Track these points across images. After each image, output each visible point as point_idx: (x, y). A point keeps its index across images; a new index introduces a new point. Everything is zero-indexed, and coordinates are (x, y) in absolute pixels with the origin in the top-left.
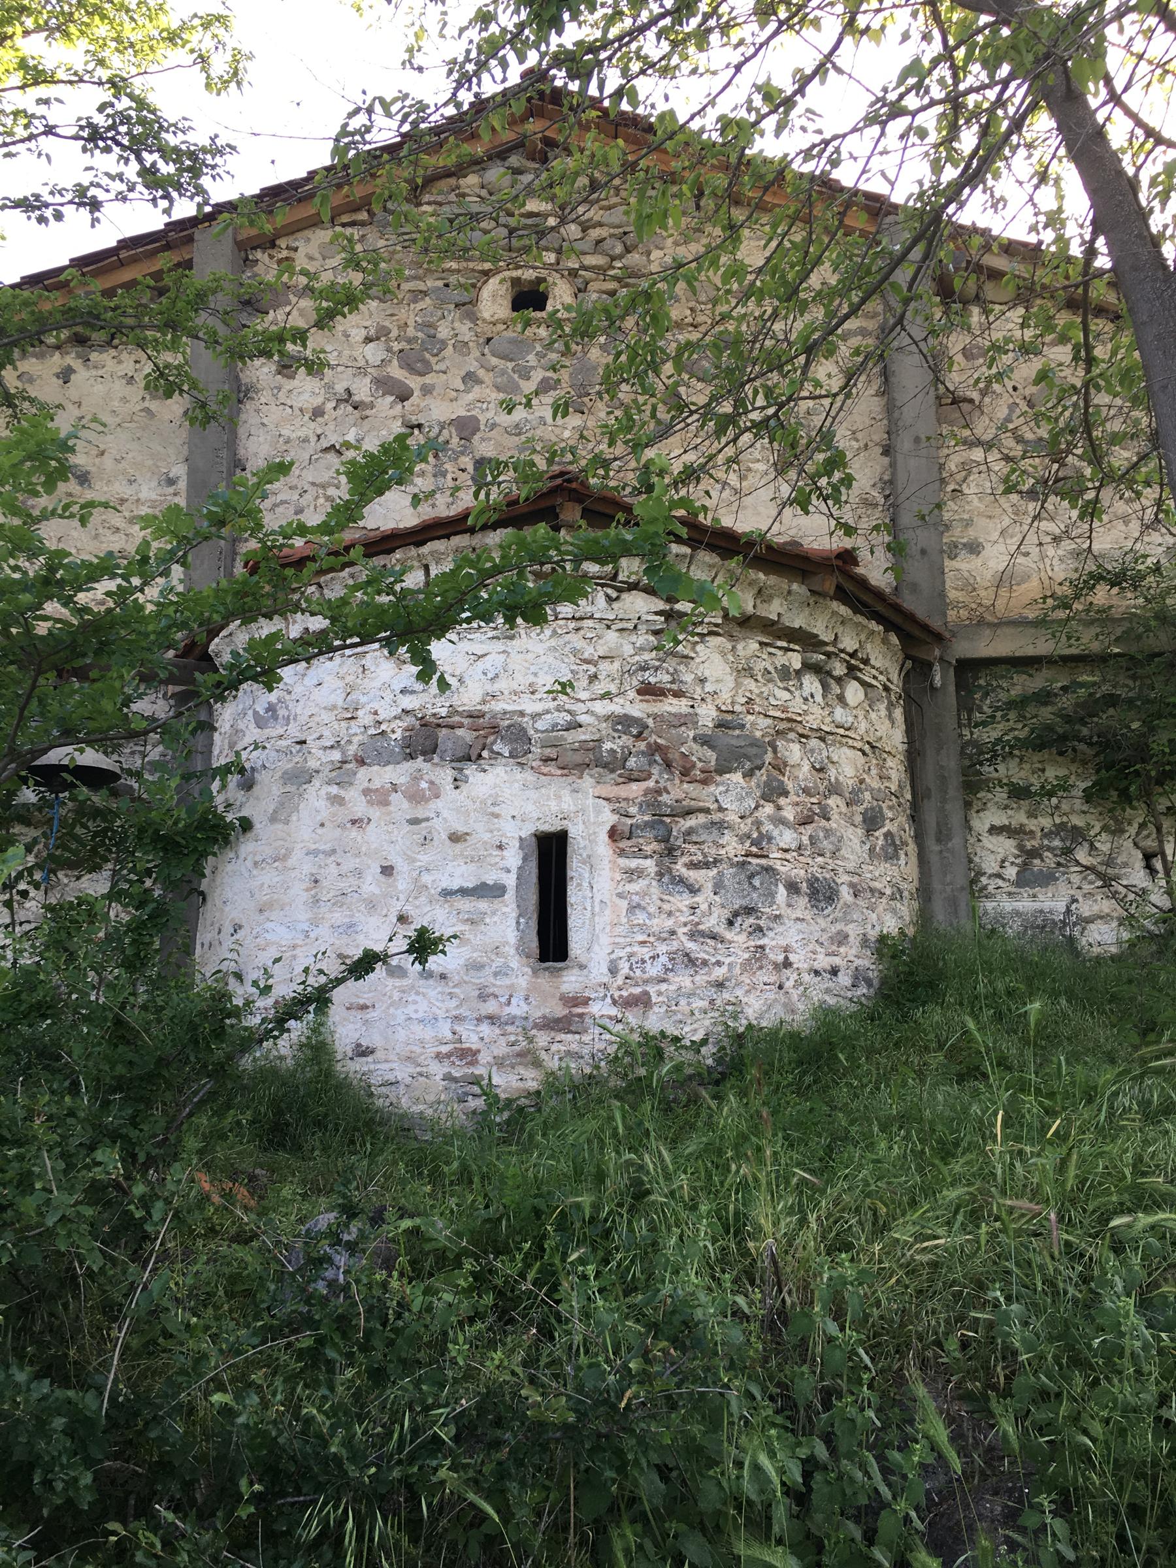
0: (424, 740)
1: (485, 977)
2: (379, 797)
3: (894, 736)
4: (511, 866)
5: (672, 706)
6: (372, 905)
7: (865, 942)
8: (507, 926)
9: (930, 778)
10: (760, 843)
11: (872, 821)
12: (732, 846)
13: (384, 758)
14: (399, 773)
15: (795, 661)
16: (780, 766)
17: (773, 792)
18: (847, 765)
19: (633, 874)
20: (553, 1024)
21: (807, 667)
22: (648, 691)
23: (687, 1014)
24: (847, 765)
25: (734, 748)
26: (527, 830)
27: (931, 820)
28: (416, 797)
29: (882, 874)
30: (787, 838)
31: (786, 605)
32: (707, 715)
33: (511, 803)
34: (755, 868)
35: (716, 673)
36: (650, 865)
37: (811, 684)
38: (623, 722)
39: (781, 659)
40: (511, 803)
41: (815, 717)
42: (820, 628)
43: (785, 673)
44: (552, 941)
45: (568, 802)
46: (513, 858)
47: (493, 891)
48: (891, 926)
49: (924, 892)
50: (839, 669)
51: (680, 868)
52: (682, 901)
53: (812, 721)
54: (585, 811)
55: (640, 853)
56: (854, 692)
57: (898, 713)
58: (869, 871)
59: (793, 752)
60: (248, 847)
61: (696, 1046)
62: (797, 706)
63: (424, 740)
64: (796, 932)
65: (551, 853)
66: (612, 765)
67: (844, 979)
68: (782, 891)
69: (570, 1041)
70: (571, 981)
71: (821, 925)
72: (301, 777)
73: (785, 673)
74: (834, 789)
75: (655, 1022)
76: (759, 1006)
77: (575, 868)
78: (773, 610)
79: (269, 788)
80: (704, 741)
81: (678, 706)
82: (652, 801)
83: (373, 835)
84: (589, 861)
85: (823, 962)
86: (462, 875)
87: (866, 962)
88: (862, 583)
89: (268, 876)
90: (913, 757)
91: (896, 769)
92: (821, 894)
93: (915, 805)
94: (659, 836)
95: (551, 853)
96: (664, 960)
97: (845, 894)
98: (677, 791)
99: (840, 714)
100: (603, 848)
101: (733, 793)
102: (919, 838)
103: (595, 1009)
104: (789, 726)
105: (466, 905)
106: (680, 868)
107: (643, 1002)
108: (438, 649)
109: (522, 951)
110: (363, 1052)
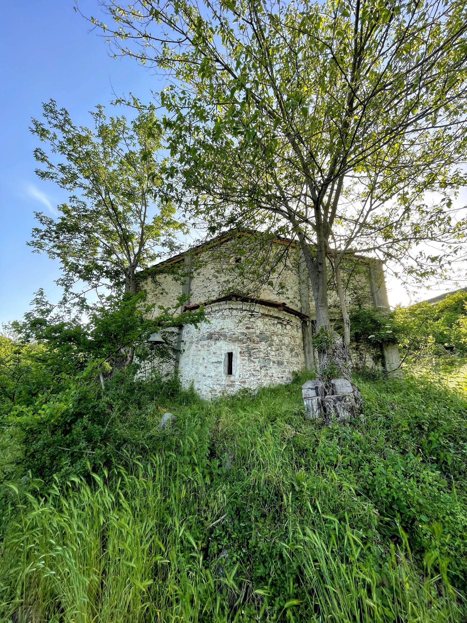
0: (210, 337)
1: (218, 377)
2: (203, 346)
3: (300, 334)
4: (223, 358)
5: (251, 330)
6: (201, 364)
7: (290, 372)
8: (222, 368)
9: (307, 342)
10: (268, 354)
11: (292, 350)
12: (262, 355)
13: (204, 340)
14: (205, 342)
15: (276, 322)
16: (272, 341)
17: (271, 345)
18: (286, 340)
19: (243, 360)
20: (228, 386)
21: (278, 323)
22: (247, 328)
23: (253, 385)
24: (286, 340)
25: (263, 338)
26: (226, 352)
27: (307, 350)
28: (208, 346)
29: (294, 360)
30: (273, 353)
31: (274, 312)
32: (258, 332)
33: (224, 347)
34: (267, 358)
35: (260, 325)
36: (247, 358)
37: (279, 326)
38: (243, 333)
39: (273, 322)
40: (224, 347)
41: (280, 332)
42: (281, 316)
43: (274, 324)
44: (230, 372)
45: (233, 347)
46: (223, 357)
47: (221, 362)
48: (296, 369)
49: (306, 362)
50: (285, 323)
51: (252, 359)
52: (252, 364)
53: (279, 333)
54: (236, 349)
55: (245, 356)
56: (288, 327)
57: (300, 330)
58: (290, 359)
59: (275, 338)
60: (184, 354)
61: (254, 390)
62: (276, 330)
63: (210, 337)
64: (274, 370)
65: (230, 355)
66: (241, 341)
67: (285, 379)
68: (271, 363)
69: (232, 389)
70: (232, 378)
71: (280, 369)
72: (192, 343)
73: (274, 324)
74: (284, 344)
75: (246, 386)
76: (266, 383)
77: (234, 359)
78: (271, 313)
79: (188, 344)
80: (258, 337)
81: (253, 330)
82: (247, 347)
83: (202, 353)
84: (236, 358)
85: (280, 376)
86: (214, 359)
87: (290, 376)
88: (288, 308)
89: (187, 359)
90: (304, 339)
91: (299, 341)
92: (280, 363)
93: (304, 347)
94: (249, 353)
95: (230, 355)
96: (250, 375)
97: (286, 363)
98: (252, 345)
99: (285, 331)
100: (239, 355)
101: (263, 346)
102: (305, 353)
103: (236, 383)
104: (274, 333)
105: (215, 364)
106: (252, 359)
107: (244, 382)
108: (198, 324)
109: (224, 373)
110: (199, 389)
